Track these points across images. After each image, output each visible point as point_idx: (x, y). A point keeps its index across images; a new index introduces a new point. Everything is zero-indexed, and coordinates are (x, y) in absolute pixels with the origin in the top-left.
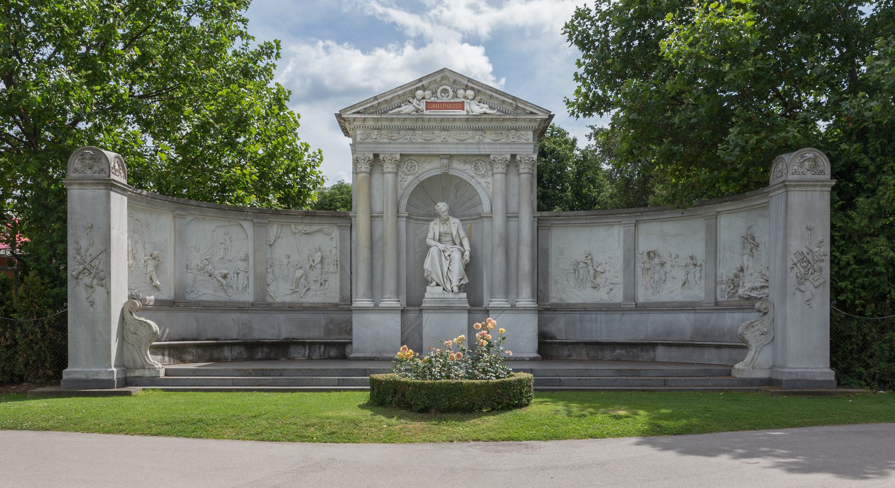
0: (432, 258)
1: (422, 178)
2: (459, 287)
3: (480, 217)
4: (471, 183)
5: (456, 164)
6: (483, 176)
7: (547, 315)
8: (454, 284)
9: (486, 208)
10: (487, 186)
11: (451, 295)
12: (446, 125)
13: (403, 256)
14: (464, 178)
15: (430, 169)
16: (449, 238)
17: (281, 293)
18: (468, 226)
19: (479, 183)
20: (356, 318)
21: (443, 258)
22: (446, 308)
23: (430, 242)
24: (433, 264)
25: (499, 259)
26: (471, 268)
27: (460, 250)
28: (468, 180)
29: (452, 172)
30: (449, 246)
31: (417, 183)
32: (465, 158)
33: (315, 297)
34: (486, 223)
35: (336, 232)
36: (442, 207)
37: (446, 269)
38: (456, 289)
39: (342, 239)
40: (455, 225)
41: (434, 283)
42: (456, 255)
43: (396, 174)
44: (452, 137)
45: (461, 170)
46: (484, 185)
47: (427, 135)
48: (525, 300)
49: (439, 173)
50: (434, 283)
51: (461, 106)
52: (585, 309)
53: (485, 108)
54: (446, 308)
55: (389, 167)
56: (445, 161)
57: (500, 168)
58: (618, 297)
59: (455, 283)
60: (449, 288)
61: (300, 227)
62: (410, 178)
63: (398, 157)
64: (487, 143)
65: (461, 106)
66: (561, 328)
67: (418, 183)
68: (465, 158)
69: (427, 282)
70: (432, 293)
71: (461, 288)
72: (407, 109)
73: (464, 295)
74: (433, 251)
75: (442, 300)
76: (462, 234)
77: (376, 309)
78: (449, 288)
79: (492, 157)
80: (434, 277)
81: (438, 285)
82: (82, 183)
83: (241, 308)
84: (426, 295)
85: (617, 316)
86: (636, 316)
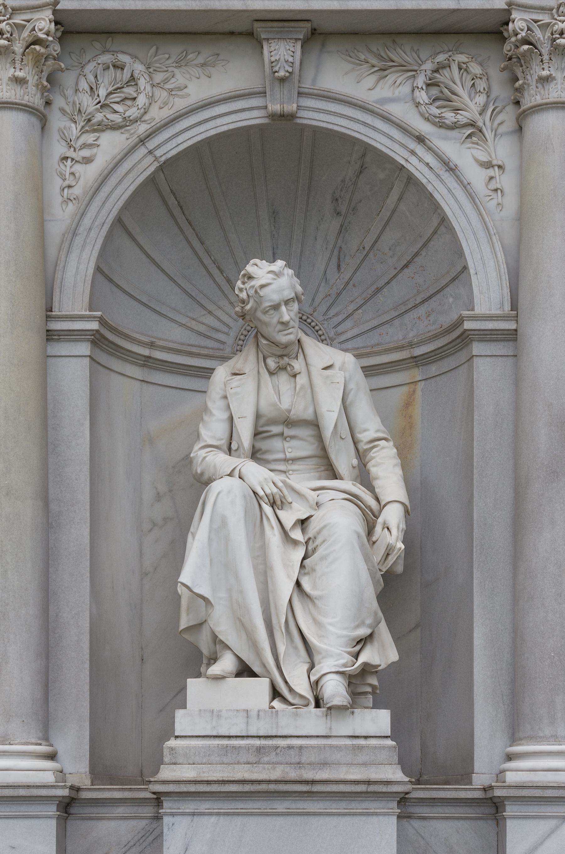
0: (220, 527)
1: (172, 144)
2: (356, 680)
3: (458, 341)
4: (415, 167)
5: (339, 76)
6: (473, 131)
8: (325, 666)
9: (487, 293)
11: (312, 722)
13: (76, 534)
14: (380, 142)
16: (301, 446)
18: (396, 397)
19: (451, 169)
21: (274, 537)
24: (222, 562)
27: (354, 499)
28: (399, 155)
29: (317, 115)
30: (304, 481)
31: (143, 167)
37: (284, 588)
38: (335, 690)
40: (330, 377)
41: (226, 664)
42: (339, 521)
43: (41, 117)
46: (476, 177)
49: (255, 118)
50: (226, 664)
56: (282, 52)
59: (334, 658)
60: (301, 685)
62: (110, 144)
63: (44, 22)
67: (148, 167)
69: (193, 656)
70: (216, 709)
73: (378, 721)
74: (226, 498)
75: (265, 745)
76: (370, 426)
78: (301, 685)
79: (519, 22)
80: (222, 624)
81: (245, 671)
84: (183, 722)
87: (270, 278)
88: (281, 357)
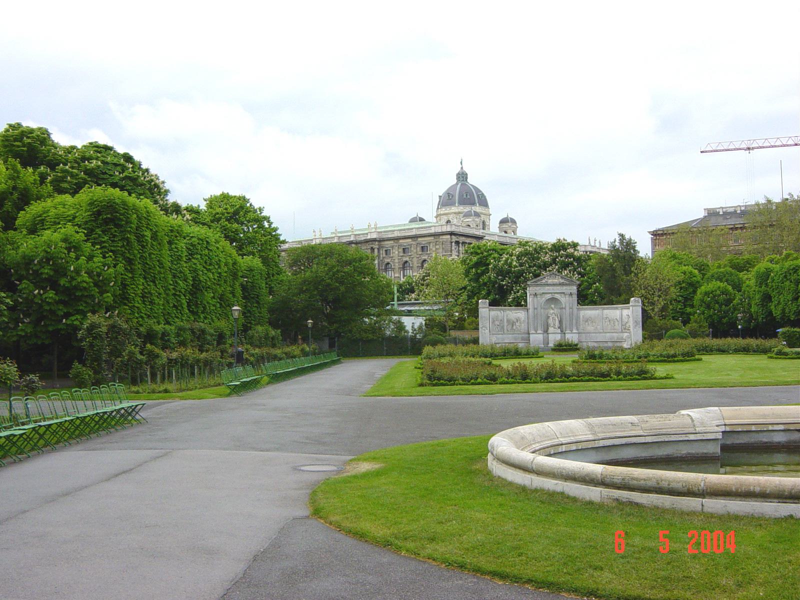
10: (563, 300)
20: (531, 335)
26: (560, 322)
34: (564, 310)
39: (525, 314)
44: (555, 288)
47: (548, 287)
71: (559, 328)
72: (544, 281)
74: (551, 318)
77: (537, 333)
86: (603, 334)
87: (553, 306)
88: (553, 309)
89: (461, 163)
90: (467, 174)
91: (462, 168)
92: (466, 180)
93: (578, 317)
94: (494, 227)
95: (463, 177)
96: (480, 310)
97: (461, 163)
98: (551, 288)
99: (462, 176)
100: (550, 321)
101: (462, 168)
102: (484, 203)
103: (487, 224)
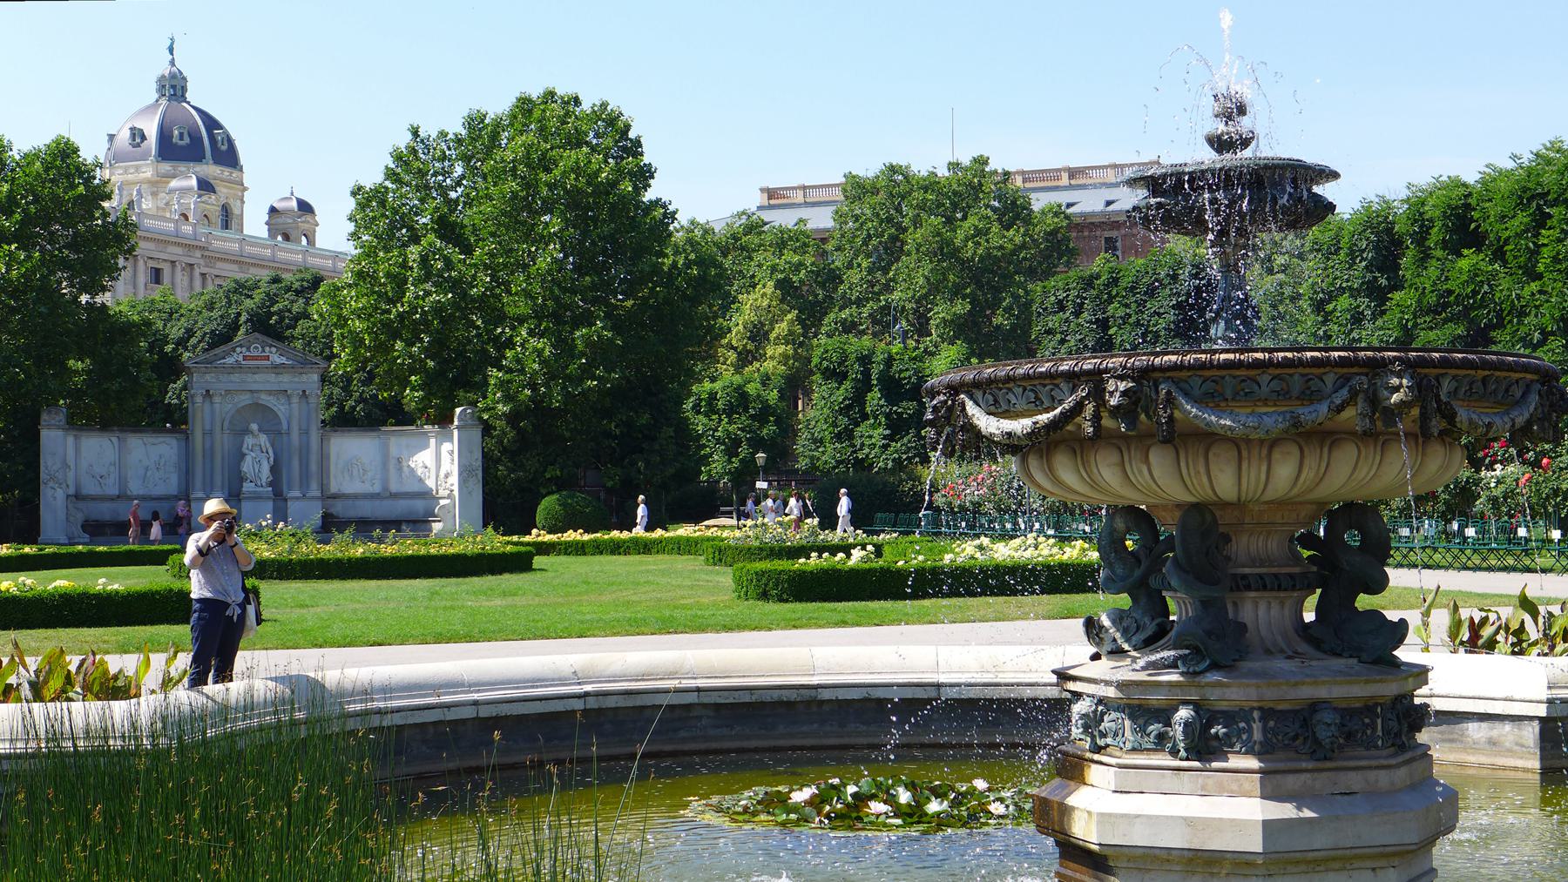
7: (330, 501)
9: (285, 426)
12: (257, 370)
15: (245, 399)
17: (135, 488)
22: (257, 497)
23: (244, 450)
25: (296, 463)
26: (275, 469)
32: (270, 393)
33: (160, 490)
35: (174, 442)
36: (254, 427)
45: (265, 399)
48: (315, 491)
51: (268, 358)
52: (356, 497)
53: (283, 360)
54: (257, 497)
55: (217, 399)
57: (295, 400)
58: (377, 488)
61: (152, 440)
64: (286, 380)
65: (268, 358)
66: (339, 509)
68: (270, 393)
70: (247, 487)
71: (271, 484)
72: (230, 360)
74: (248, 459)
82: (49, 427)
83: (112, 499)
85: (377, 502)
89: (171, 50)
90: (185, 79)
91: (172, 63)
92: (183, 96)
93: (324, 458)
94: (255, 224)
95: (174, 87)
96: (44, 433)
97: (171, 50)
98: (250, 378)
99: (173, 87)
100: (247, 466)
101: (172, 63)
102: (228, 156)
103: (236, 211)
